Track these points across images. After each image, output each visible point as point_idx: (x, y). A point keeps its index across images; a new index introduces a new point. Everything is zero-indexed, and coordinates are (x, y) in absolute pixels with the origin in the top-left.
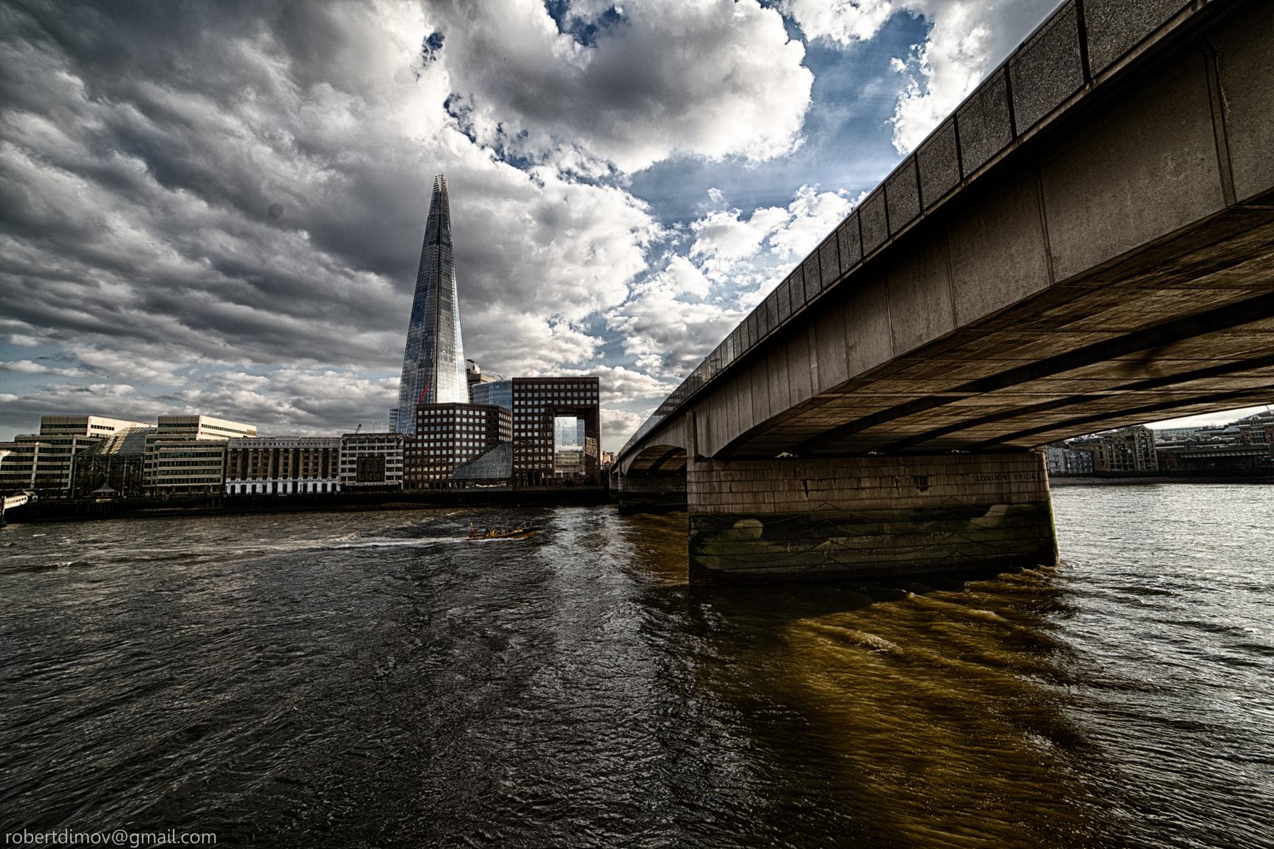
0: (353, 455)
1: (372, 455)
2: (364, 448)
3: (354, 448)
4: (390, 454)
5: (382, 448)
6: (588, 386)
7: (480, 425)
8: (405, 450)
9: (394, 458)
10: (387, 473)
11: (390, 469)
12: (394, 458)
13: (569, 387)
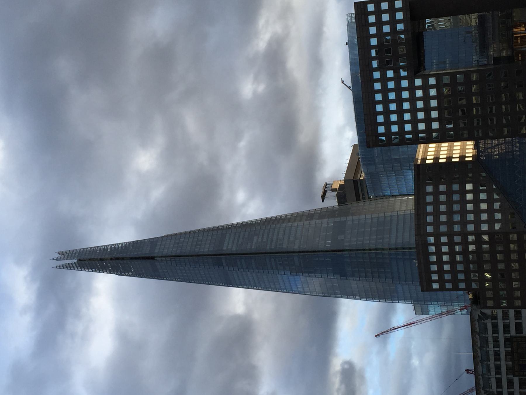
0: (510, 383)
1: (507, 353)
2: (498, 368)
3: (499, 382)
4: (506, 328)
5: (496, 341)
6: (372, 19)
7: (449, 193)
8: (498, 306)
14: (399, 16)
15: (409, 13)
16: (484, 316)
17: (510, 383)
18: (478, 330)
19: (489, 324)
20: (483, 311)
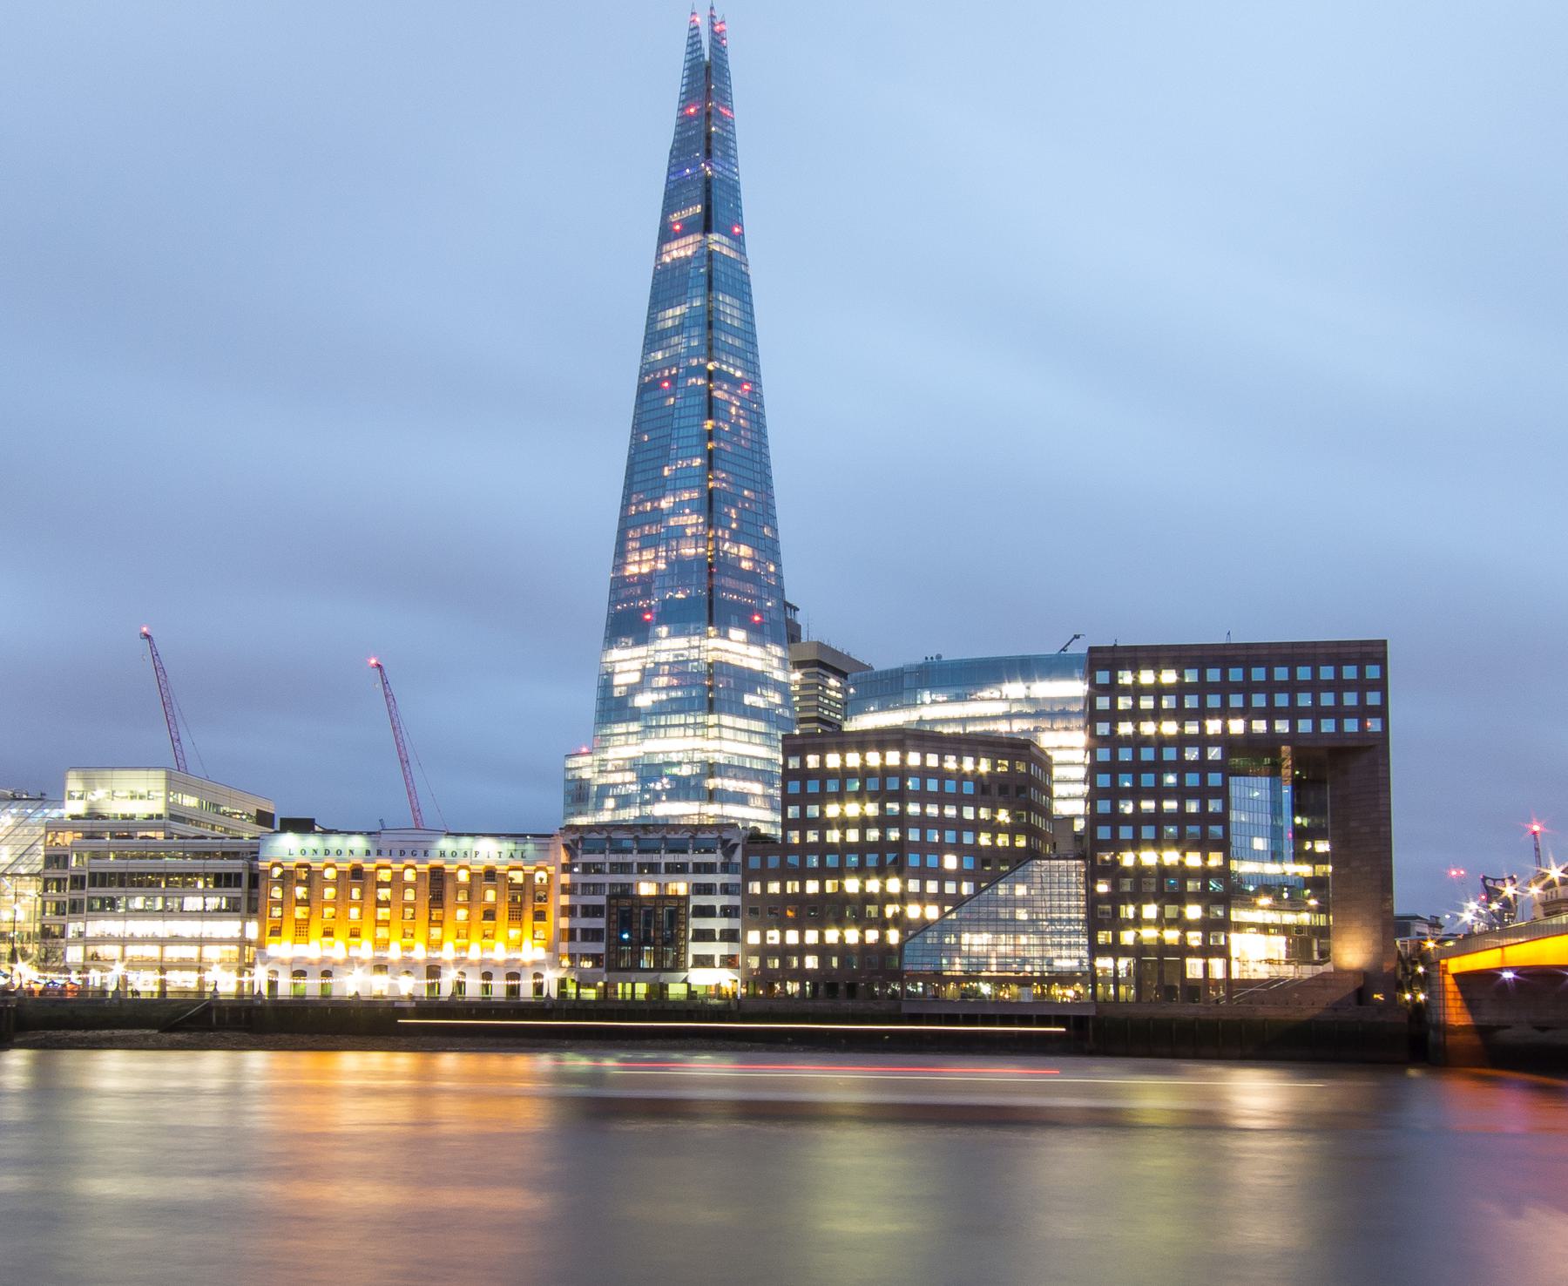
0: (596, 888)
6: (1350, 672)
9: (718, 901)
10: (696, 948)
11: (704, 936)
12: (718, 901)
13: (1281, 674)
14: (1351, 726)
15: (1354, 744)
16: (729, 849)
17: (596, 888)
18: (700, 836)
19: (716, 858)
20: (739, 850)
